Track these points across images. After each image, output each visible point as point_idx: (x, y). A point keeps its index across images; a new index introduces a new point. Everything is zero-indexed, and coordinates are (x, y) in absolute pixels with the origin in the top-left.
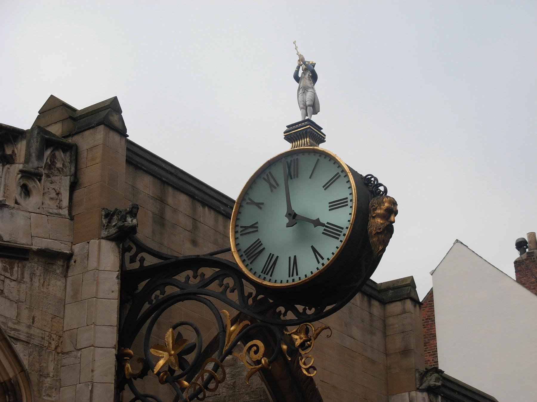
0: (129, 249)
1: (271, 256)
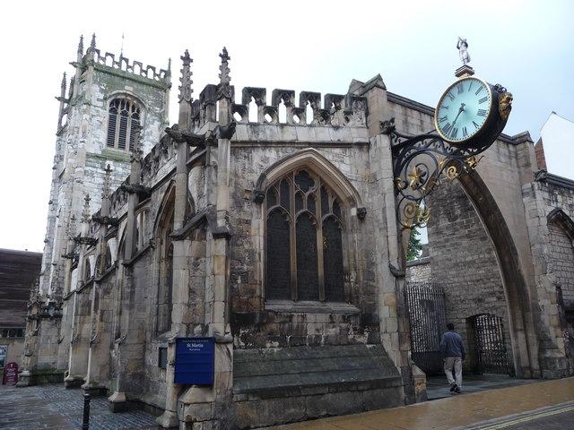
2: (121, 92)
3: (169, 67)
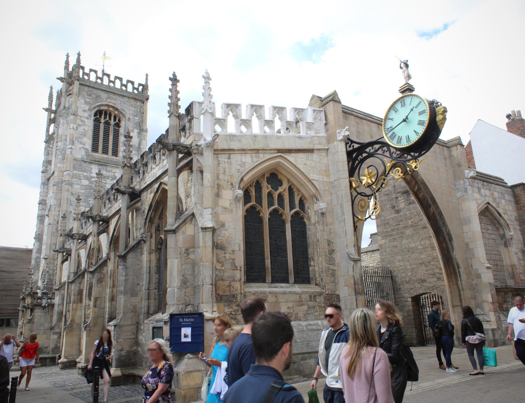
0: (348, 143)
1: (399, 137)
2: (104, 103)
3: (147, 81)
